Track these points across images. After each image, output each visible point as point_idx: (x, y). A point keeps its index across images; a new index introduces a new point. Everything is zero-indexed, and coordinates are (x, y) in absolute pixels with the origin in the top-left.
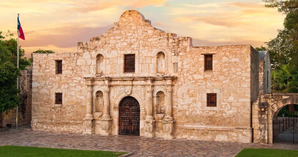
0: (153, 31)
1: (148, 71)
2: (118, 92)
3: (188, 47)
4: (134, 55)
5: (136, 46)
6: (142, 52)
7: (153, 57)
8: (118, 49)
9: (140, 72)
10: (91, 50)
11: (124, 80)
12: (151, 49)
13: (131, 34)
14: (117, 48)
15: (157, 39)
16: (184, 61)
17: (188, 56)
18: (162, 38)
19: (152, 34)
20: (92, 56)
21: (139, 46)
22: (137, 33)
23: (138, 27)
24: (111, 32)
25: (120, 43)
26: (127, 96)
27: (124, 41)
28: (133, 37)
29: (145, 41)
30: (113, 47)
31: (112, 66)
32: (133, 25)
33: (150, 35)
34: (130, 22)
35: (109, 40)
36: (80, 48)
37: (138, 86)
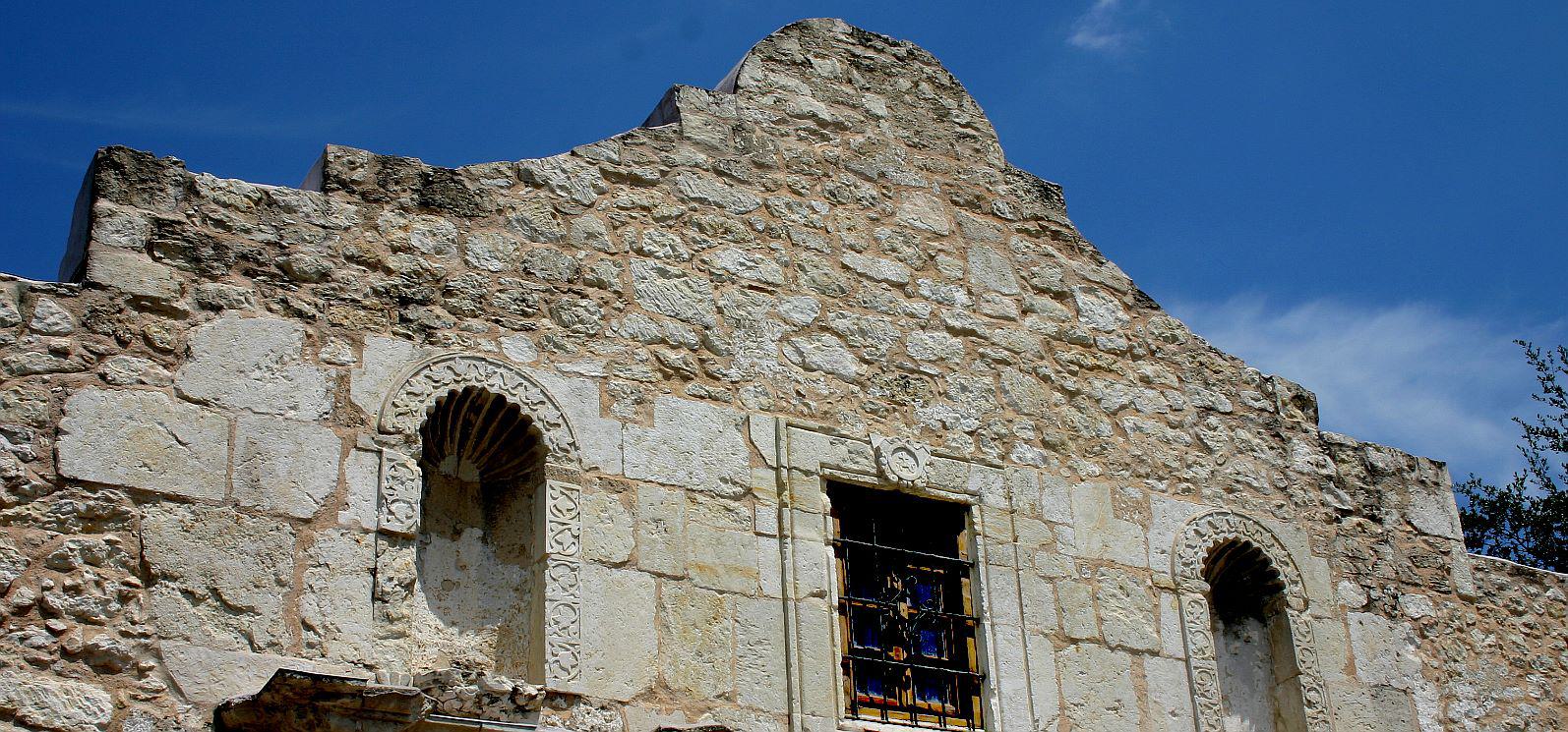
0: (1121, 314)
3: (1458, 548)
4: (951, 517)
5: (974, 424)
6: (1047, 501)
7: (1166, 580)
8: (748, 395)
10: (338, 312)
13: (889, 268)
16: (1463, 689)
17: (1476, 635)
19: (1123, 343)
20: (358, 393)
22: (960, 282)
29: (1063, 390)
30: (672, 356)
32: (908, 187)
33: (1102, 339)
36: (141, 238)
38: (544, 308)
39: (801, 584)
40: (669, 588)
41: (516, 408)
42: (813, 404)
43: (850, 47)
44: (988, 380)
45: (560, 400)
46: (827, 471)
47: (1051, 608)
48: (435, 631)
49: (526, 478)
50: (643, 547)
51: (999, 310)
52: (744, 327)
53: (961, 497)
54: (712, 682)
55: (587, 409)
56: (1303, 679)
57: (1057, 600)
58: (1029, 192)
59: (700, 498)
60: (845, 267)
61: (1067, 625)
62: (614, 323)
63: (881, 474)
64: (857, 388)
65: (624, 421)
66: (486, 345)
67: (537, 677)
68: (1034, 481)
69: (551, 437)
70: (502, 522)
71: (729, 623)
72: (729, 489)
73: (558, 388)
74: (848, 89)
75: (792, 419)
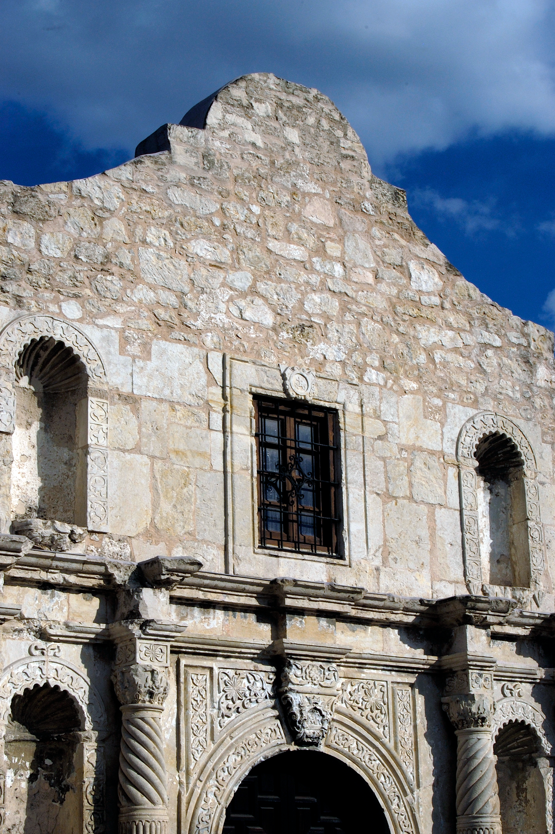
0: (437, 279)
1: (426, 558)
2: (224, 710)
8: (209, 339)
9: (377, 562)
11: (288, 602)
12: (438, 402)
14: (199, 332)
15: (470, 339)
18: (498, 342)
19: (436, 300)
21: (357, 357)
23: (346, 213)
24: (149, 189)
25: (227, 294)
26: (293, 748)
27: (253, 291)
28: (314, 279)
29: (398, 332)
30: (162, 313)
31: (164, 475)
32: (309, 194)
33: (425, 299)
34: (289, 164)
35: (131, 245)
37: (368, 673)
38: (87, 281)
39: (236, 463)
40: (159, 465)
41: (70, 350)
42: (246, 345)
43: (278, 94)
44: (353, 327)
45: (96, 343)
46: (254, 390)
47: (382, 478)
48: (17, 488)
49: (73, 392)
50: (144, 440)
51: (361, 279)
52: (206, 293)
53: (333, 406)
54: (182, 524)
55: (112, 349)
56: (530, 524)
57: (386, 472)
58: (385, 195)
59: (177, 407)
60: (269, 251)
61: (391, 488)
62: (128, 291)
63: (285, 391)
64: (271, 332)
65: (134, 358)
66: (53, 308)
67: (83, 523)
68: (377, 393)
69: (90, 367)
70: (56, 419)
71: (192, 488)
72: (193, 401)
73: (95, 335)
74: (274, 124)
75: (233, 356)
